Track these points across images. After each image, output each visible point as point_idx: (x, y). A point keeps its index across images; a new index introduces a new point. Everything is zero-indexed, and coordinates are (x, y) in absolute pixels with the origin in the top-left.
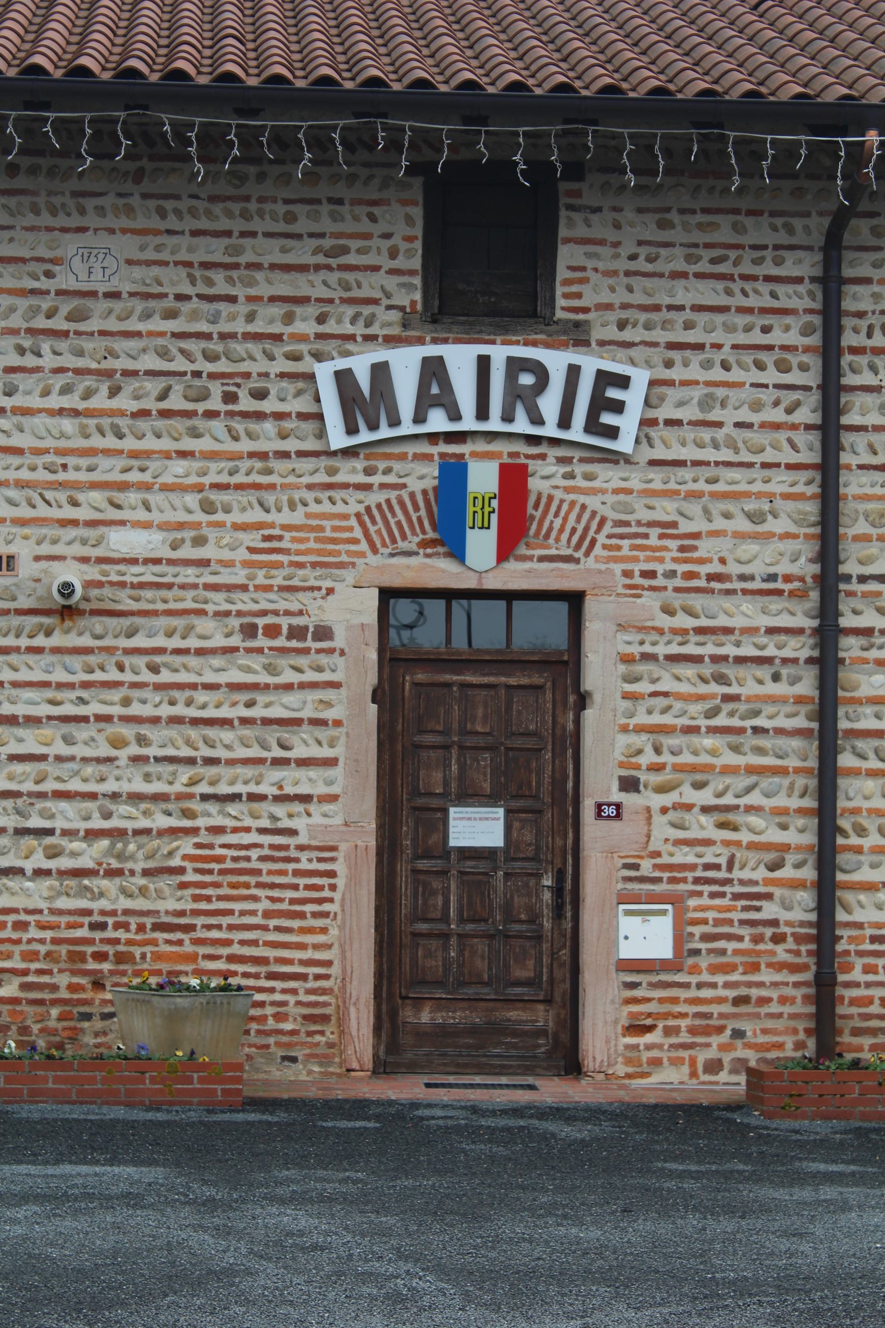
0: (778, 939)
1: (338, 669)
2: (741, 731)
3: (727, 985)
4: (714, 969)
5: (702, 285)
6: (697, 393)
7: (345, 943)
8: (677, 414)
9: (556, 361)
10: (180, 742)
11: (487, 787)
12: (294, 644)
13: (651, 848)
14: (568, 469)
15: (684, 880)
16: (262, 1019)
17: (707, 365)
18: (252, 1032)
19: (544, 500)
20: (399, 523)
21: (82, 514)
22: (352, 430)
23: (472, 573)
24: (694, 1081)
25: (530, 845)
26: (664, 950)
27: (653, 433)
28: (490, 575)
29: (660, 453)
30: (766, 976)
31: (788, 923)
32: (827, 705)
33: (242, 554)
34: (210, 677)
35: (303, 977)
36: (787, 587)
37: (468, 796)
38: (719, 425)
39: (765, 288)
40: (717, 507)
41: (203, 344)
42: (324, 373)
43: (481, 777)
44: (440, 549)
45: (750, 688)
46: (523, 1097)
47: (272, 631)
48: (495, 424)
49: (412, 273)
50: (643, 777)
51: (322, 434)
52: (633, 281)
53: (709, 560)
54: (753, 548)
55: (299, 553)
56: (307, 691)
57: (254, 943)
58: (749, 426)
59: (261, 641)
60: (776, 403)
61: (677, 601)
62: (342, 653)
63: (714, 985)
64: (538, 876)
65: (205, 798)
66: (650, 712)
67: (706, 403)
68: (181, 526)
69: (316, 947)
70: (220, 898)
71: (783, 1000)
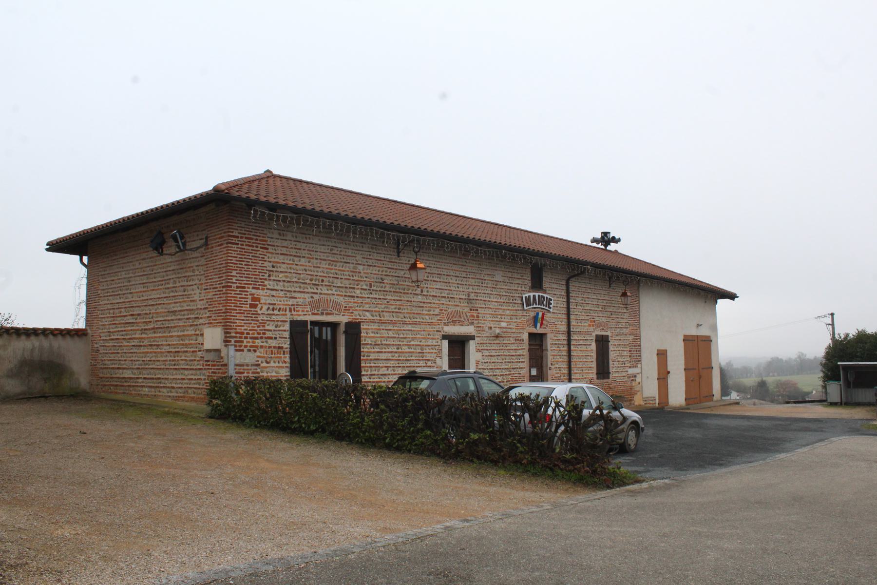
9: (545, 296)
32: (569, 351)
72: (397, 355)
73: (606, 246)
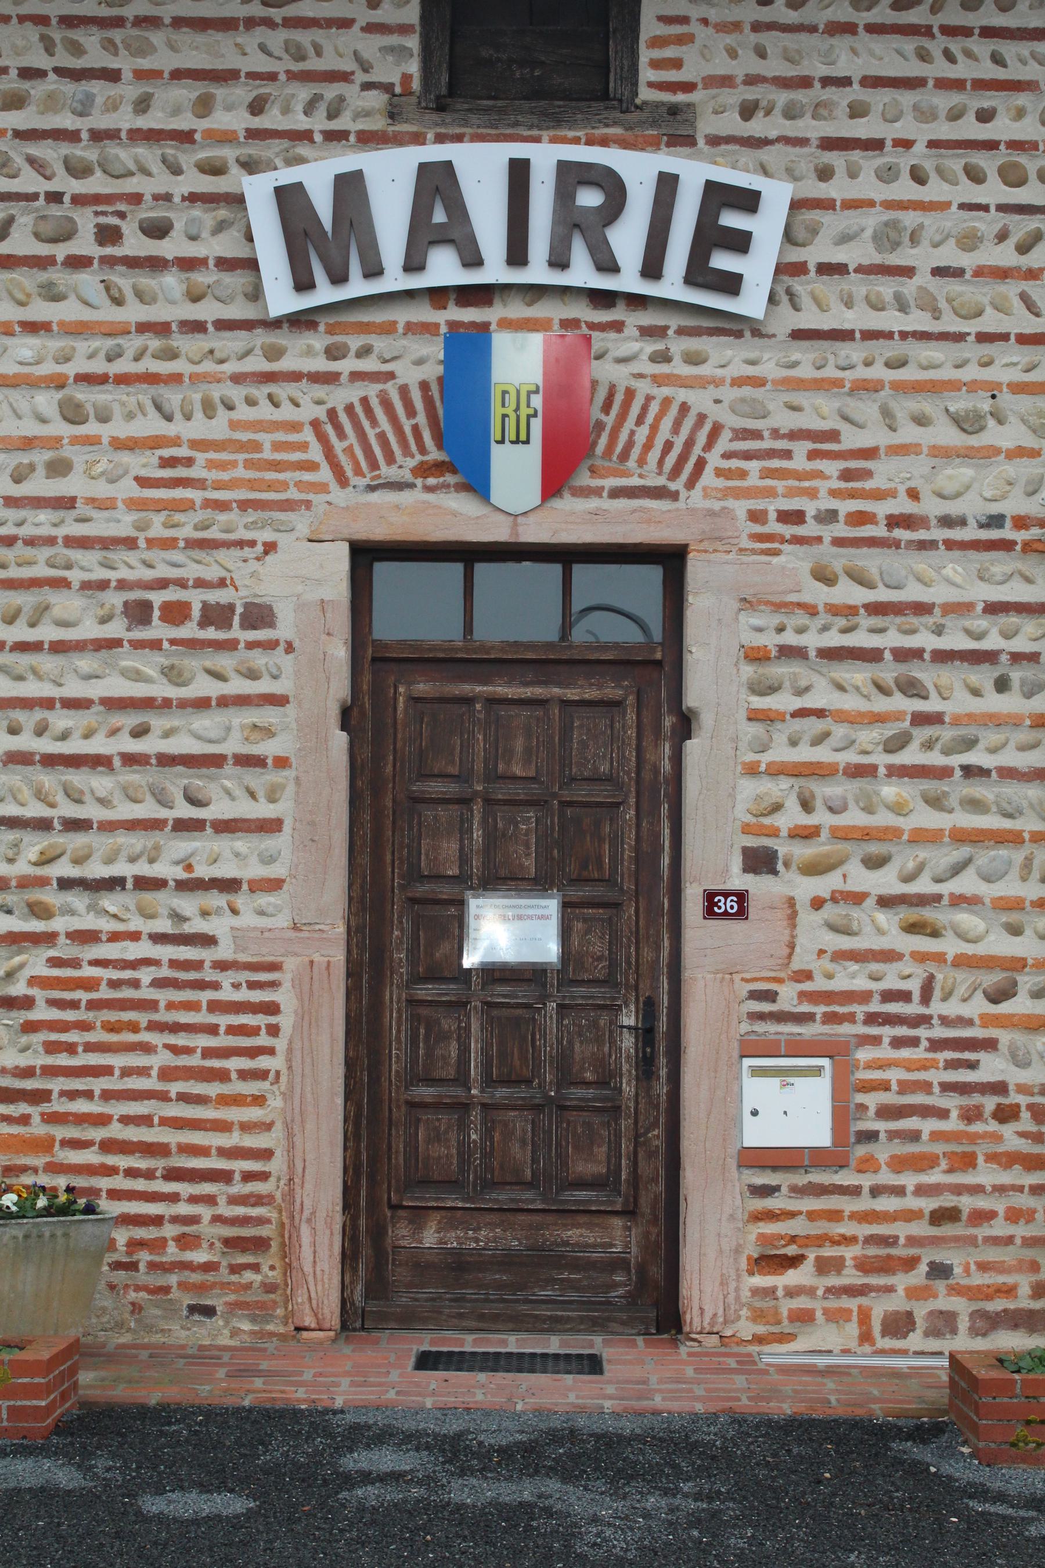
0: (1006, 1114)
1: (283, 675)
2: (945, 773)
3: (921, 1190)
4: (899, 1164)
5: (879, 44)
6: (871, 220)
8: (838, 256)
9: (638, 169)
10: (26, 794)
11: (530, 864)
12: (211, 633)
13: (796, 965)
14: (659, 346)
15: (851, 1018)
16: (159, 1245)
17: (888, 175)
18: (142, 1266)
19: (619, 398)
20: (382, 437)
22: (303, 284)
23: (502, 517)
24: (867, 1348)
25: (599, 959)
26: (817, 1132)
27: (798, 285)
28: (532, 519)
29: (810, 319)
30: (986, 1175)
31: (1022, 1089)
33: (128, 489)
34: (74, 689)
35: (225, 1177)
36: (1020, 536)
37: (499, 879)
38: (908, 272)
39: (982, 48)
40: (904, 407)
41: (66, 149)
42: (258, 192)
43: (521, 849)
44: (450, 479)
46: (563, 1395)
47: (176, 613)
49: (404, 29)
50: (783, 848)
51: (256, 294)
52: (766, 38)
53: (892, 494)
54: (963, 472)
55: (219, 486)
56: (232, 711)
57: (146, 1120)
58: (957, 273)
59: (158, 630)
60: (1002, 236)
61: (839, 560)
62: (290, 648)
63: (899, 1191)
64: (615, 1010)
65: (65, 884)
66: (794, 743)
67: (888, 237)
68: (28, 443)
69: (246, 1127)
70: (89, 1047)
71: (1014, 1215)
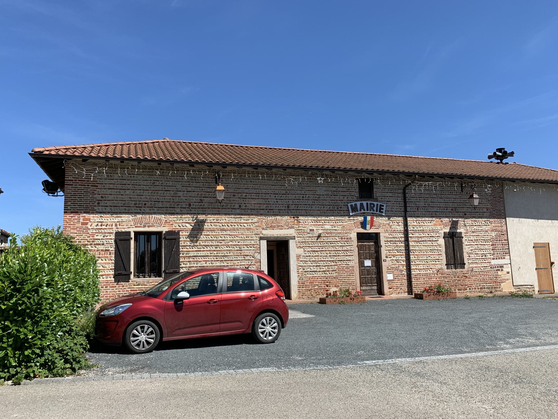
7: (356, 278)
9: (375, 203)
21: (321, 223)
45: (399, 245)
48: (369, 211)
67: (391, 208)
72: (215, 252)
73: (501, 160)
